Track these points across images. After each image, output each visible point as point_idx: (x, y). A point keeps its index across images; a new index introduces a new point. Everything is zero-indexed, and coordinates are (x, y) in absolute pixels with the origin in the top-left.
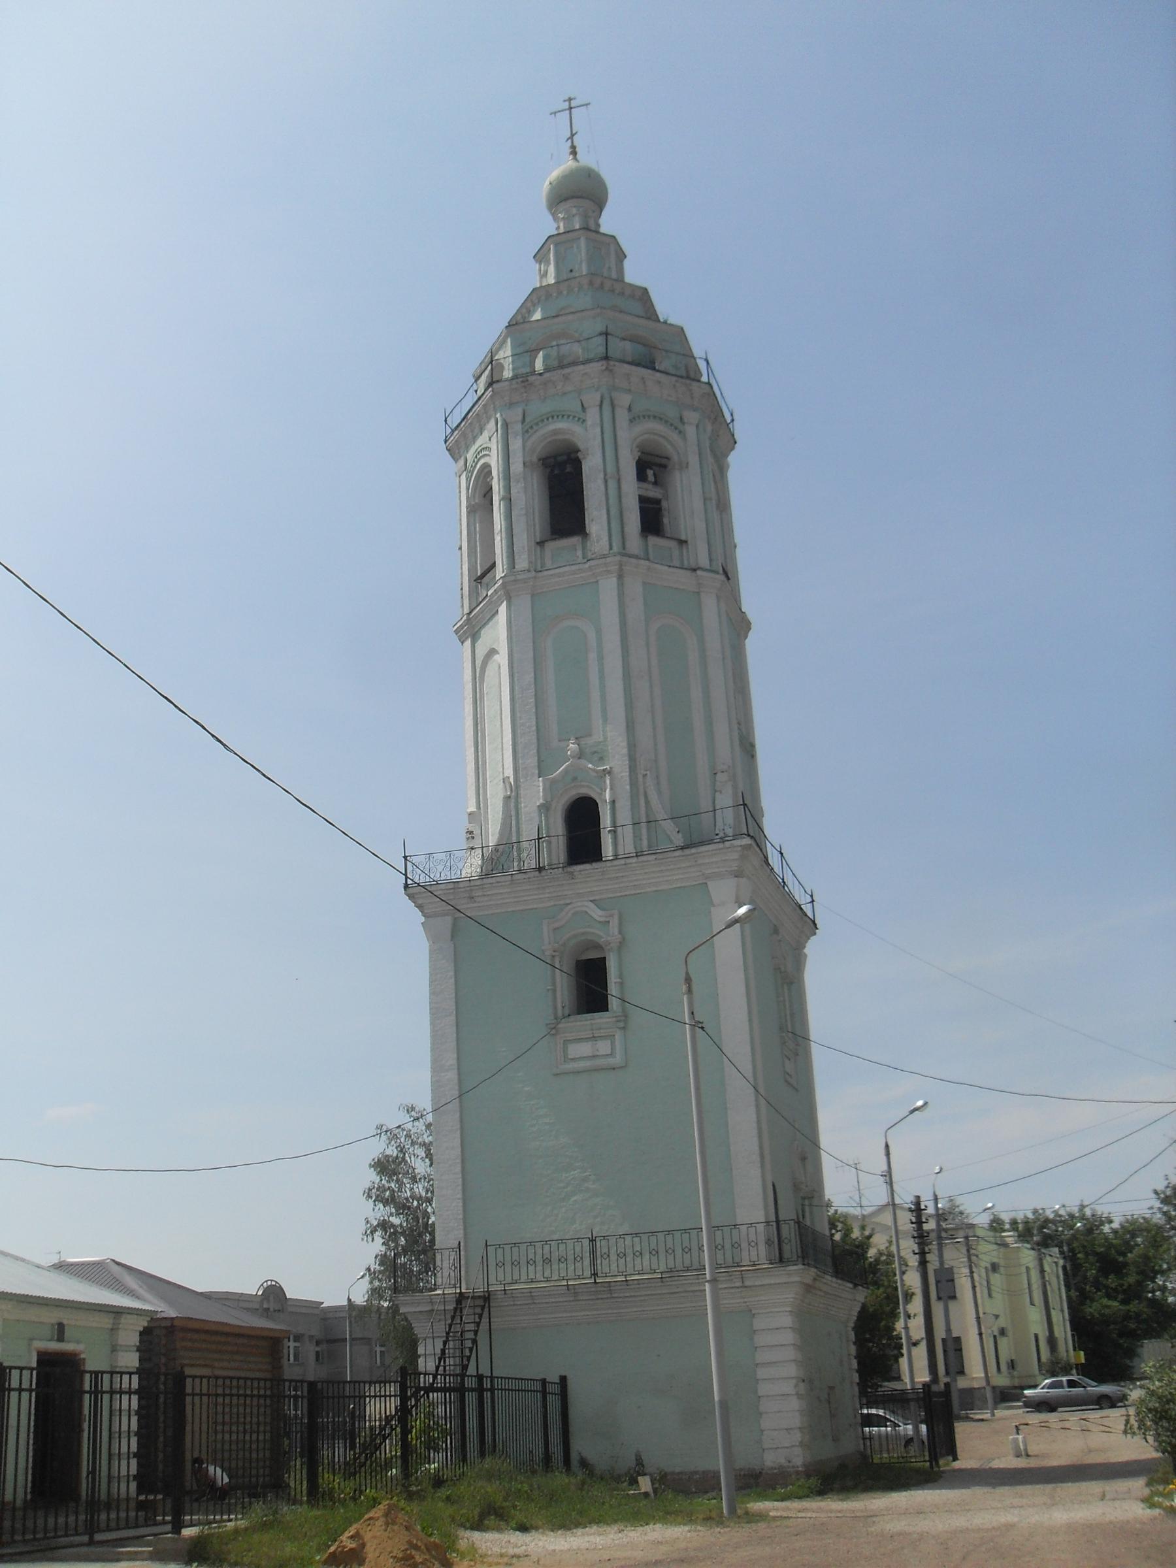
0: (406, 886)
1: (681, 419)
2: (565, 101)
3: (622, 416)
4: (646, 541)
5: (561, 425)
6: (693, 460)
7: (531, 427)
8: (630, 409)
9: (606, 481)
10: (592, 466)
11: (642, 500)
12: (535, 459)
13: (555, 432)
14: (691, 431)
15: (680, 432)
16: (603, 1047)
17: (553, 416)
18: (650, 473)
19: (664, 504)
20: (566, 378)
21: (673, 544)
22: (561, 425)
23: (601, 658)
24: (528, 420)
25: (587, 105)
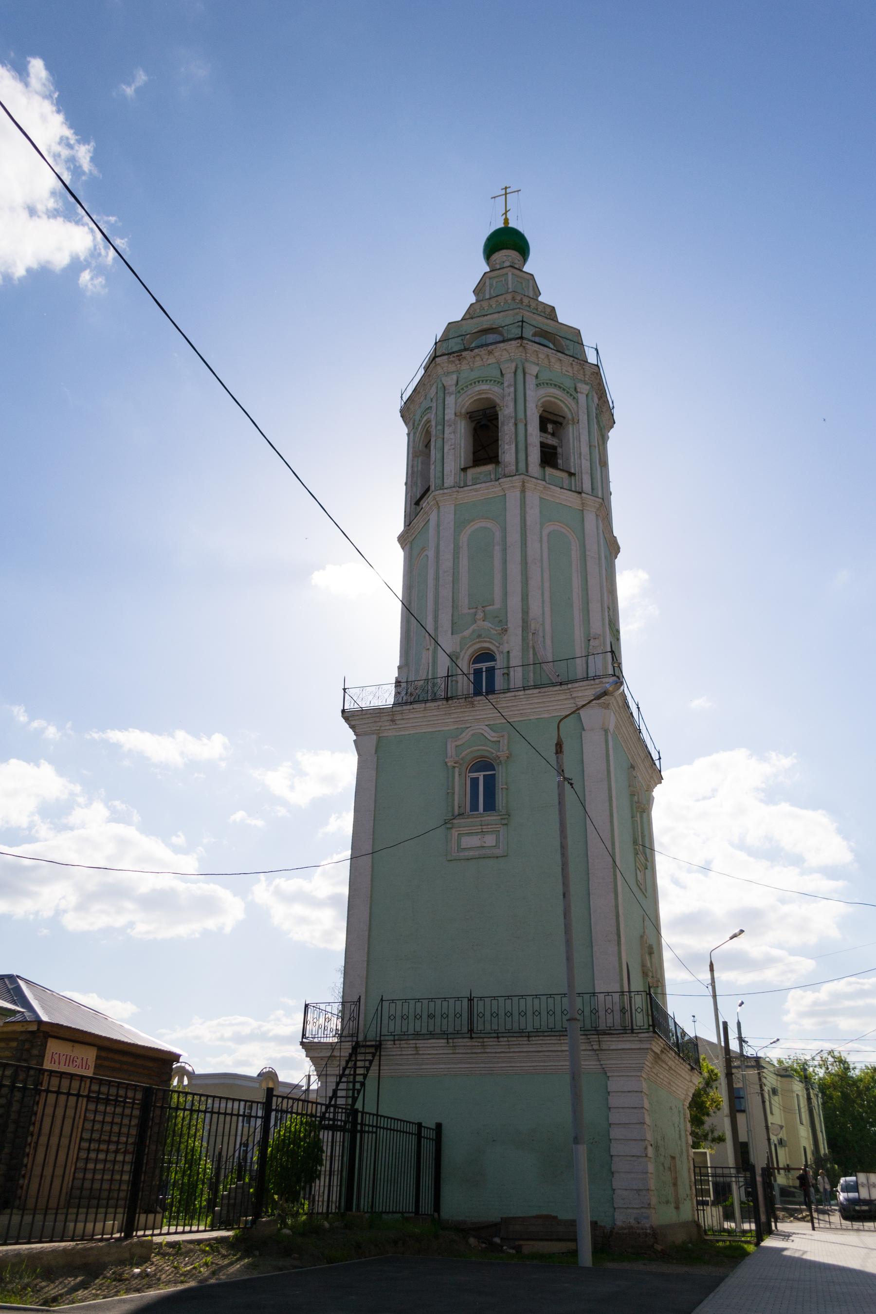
0: (343, 711)
1: (575, 389)
2: (502, 189)
3: (531, 382)
4: (544, 471)
6: (583, 418)
7: (462, 389)
8: (537, 377)
9: (516, 424)
11: (543, 445)
12: (463, 411)
13: (480, 393)
14: (582, 398)
15: (574, 398)
16: (490, 840)
17: (479, 381)
18: (550, 427)
19: (559, 450)
20: (490, 353)
21: (564, 475)
22: (484, 387)
23: (504, 550)
24: (460, 384)
25: (518, 191)
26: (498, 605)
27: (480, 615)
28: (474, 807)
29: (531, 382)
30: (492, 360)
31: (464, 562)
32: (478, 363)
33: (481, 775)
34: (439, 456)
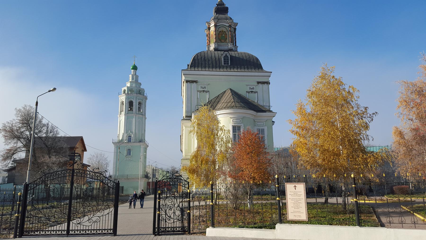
3: (138, 99)
10: (134, 104)
14: (144, 101)
20: (133, 94)
22: (131, 99)
28: (128, 155)
29: (138, 99)
33: (129, 151)
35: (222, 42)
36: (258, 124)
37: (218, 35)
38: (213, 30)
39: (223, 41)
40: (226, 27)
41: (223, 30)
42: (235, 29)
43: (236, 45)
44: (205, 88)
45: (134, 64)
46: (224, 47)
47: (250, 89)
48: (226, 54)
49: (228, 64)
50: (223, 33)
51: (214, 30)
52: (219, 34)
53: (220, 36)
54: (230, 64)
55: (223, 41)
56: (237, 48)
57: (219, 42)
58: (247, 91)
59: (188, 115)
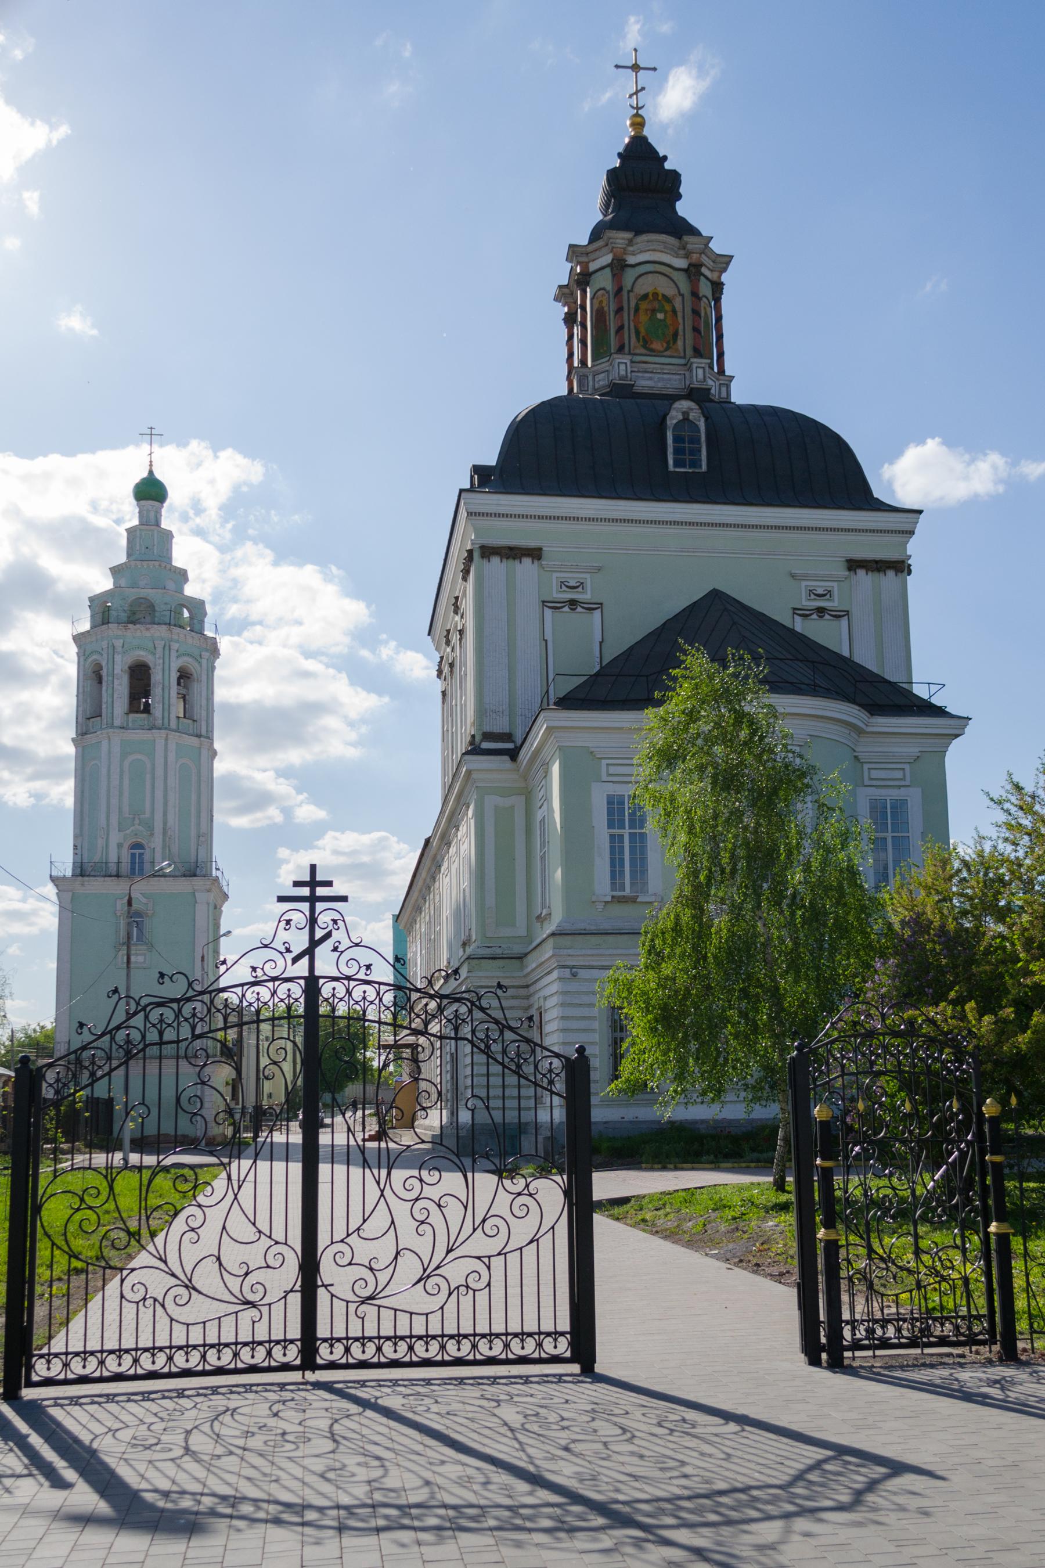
5: (142, 653)
9: (163, 689)
10: (156, 676)
12: (126, 668)
13: (139, 656)
14: (204, 662)
20: (147, 629)
21: (190, 722)
22: (142, 653)
26: (147, 815)
27: (137, 821)
29: (174, 654)
30: (148, 634)
31: (126, 782)
32: (138, 634)
34: (110, 700)
35: (653, 352)
36: (875, 774)
37: (632, 317)
38: (603, 289)
39: (657, 345)
40: (675, 275)
41: (661, 290)
42: (718, 288)
43: (722, 371)
44: (580, 589)
45: (151, 472)
46: (663, 379)
47: (813, 597)
48: (686, 418)
49: (696, 463)
50: (656, 305)
51: (609, 287)
52: (637, 310)
53: (643, 318)
54: (704, 468)
55: (657, 345)
56: (728, 387)
57: (638, 351)
58: (795, 609)
59: (497, 729)
